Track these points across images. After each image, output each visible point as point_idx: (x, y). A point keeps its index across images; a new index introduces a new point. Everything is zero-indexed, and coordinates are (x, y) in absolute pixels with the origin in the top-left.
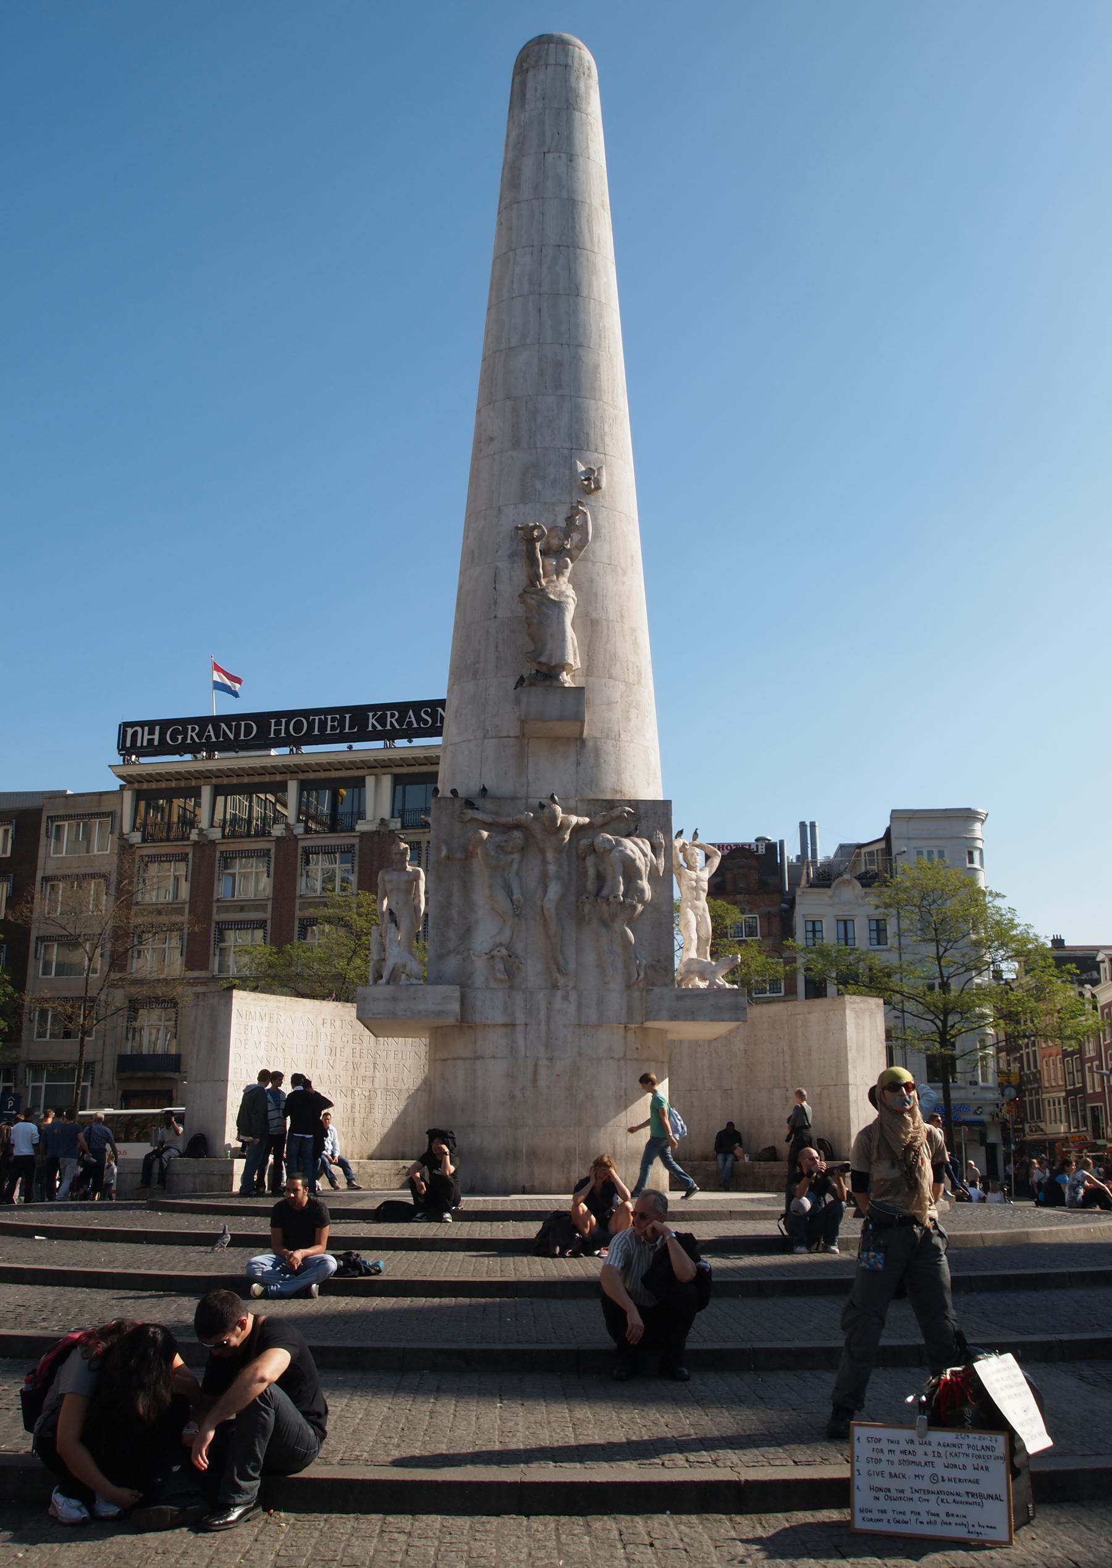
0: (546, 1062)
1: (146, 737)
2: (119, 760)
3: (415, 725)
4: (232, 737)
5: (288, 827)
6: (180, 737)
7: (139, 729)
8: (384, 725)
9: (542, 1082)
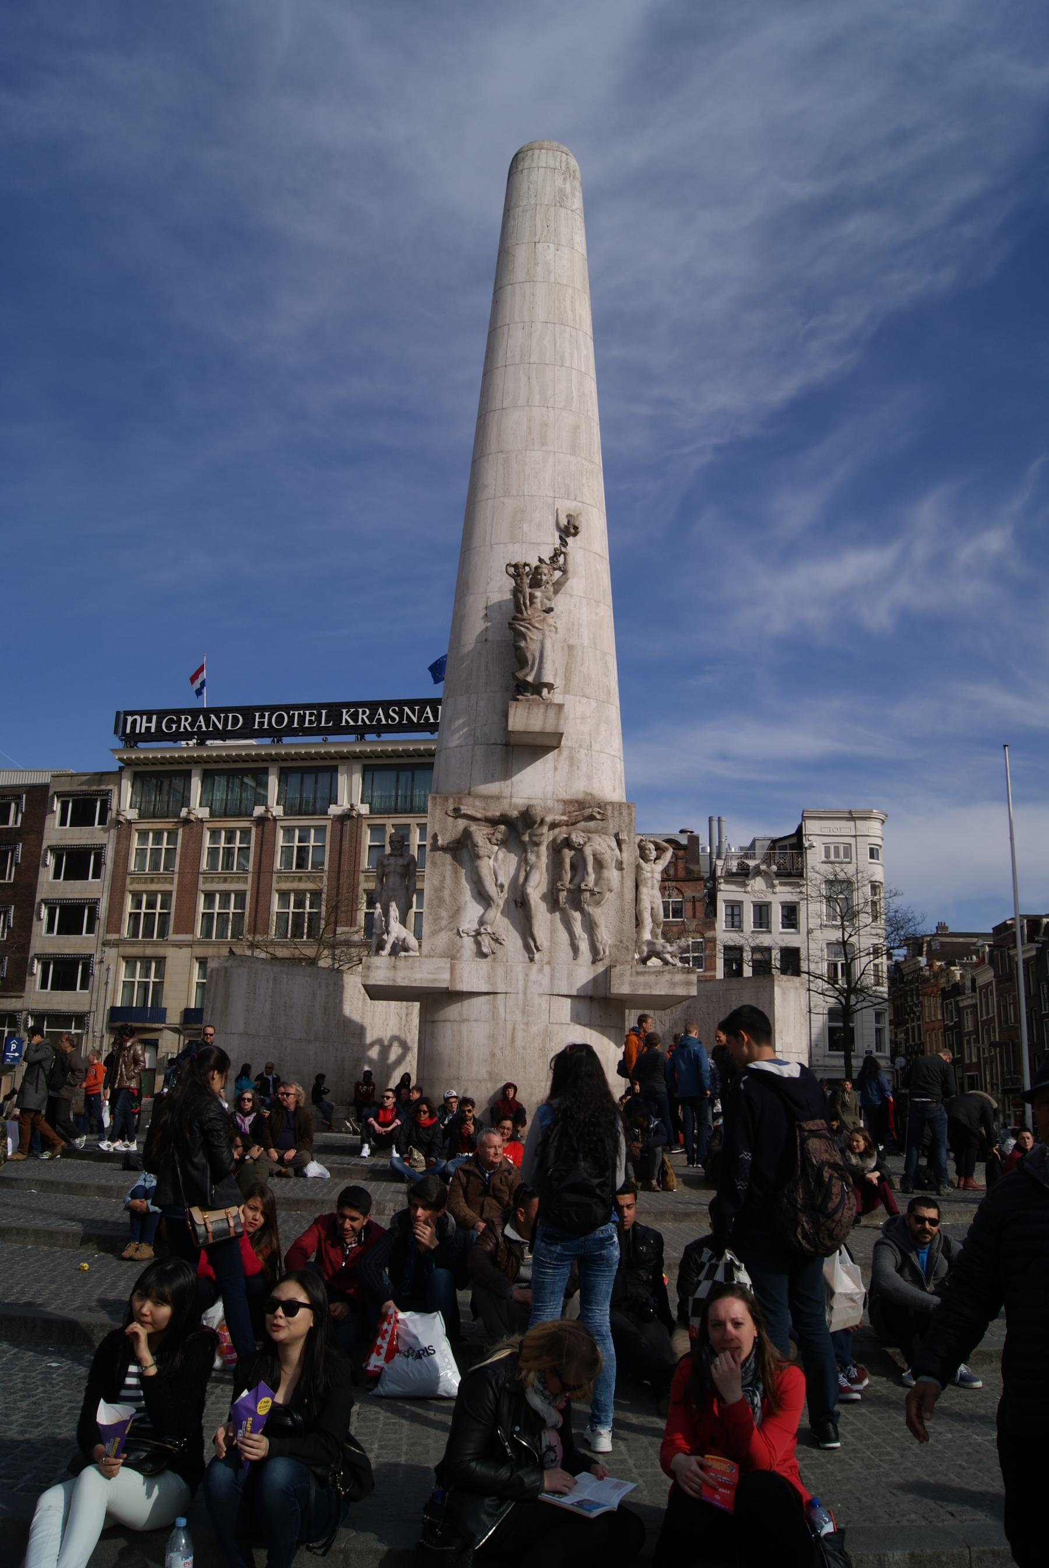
0: (522, 1026)
1: (144, 725)
3: (384, 722)
4: (220, 727)
6: (174, 726)
7: (138, 718)
8: (356, 720)
9: (519, 1043)
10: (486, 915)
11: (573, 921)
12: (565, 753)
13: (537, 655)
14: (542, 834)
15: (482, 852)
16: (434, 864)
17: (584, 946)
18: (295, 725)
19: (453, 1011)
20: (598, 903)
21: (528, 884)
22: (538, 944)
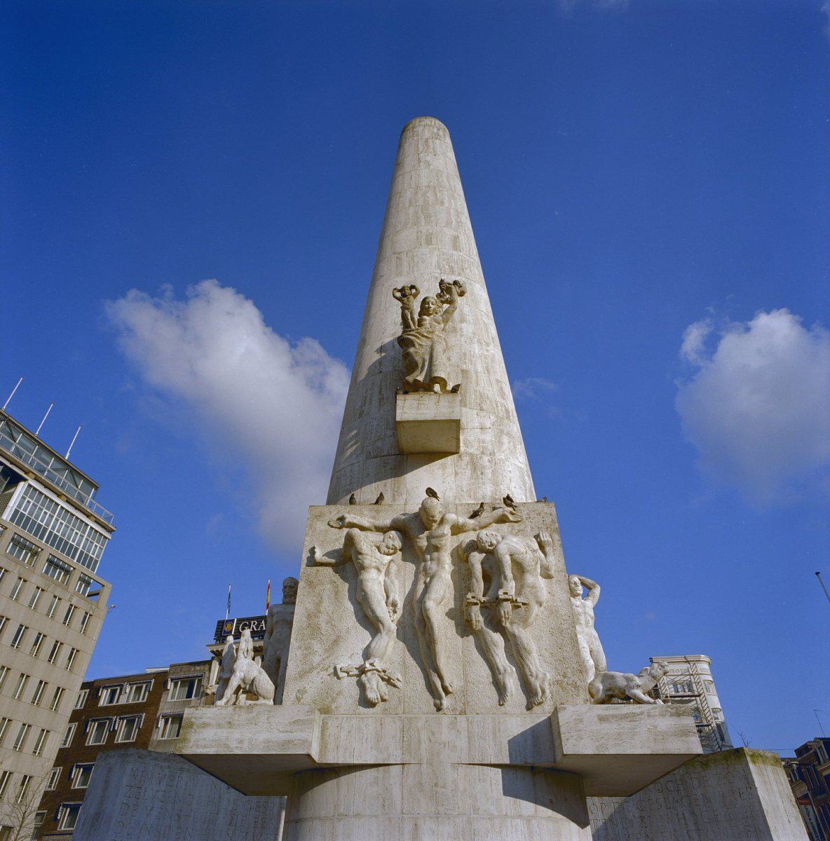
10: (373, 645)
11: (492, 647)
12: (466, 459)
13: (427, 357)
14: (443, 535)
15: (367, 561)
16: (311, 584)
17: (512, 683)
19: (326, 794)
20: (525, 622)
21: (427, 596)
22: (447, 684)
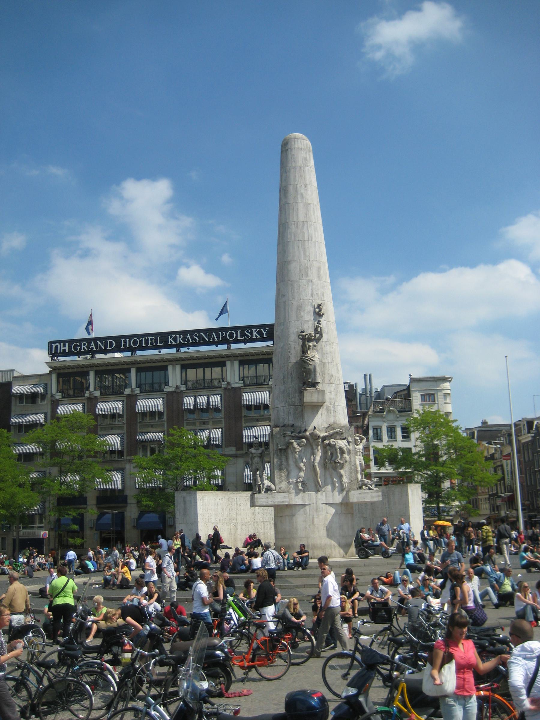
1: (62, 348)
2: (49, 359)
3: (191, 342)
4: (103, 348)
5: (132, 390)
6: (78, 348)
7: (58, 344)
8: (176, 341)
9: (315, 523)
18: (144, 345)
20: (342, 468)
